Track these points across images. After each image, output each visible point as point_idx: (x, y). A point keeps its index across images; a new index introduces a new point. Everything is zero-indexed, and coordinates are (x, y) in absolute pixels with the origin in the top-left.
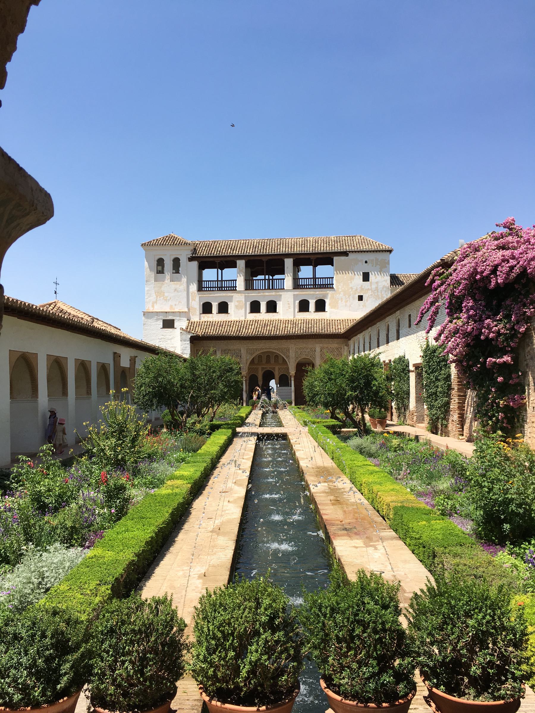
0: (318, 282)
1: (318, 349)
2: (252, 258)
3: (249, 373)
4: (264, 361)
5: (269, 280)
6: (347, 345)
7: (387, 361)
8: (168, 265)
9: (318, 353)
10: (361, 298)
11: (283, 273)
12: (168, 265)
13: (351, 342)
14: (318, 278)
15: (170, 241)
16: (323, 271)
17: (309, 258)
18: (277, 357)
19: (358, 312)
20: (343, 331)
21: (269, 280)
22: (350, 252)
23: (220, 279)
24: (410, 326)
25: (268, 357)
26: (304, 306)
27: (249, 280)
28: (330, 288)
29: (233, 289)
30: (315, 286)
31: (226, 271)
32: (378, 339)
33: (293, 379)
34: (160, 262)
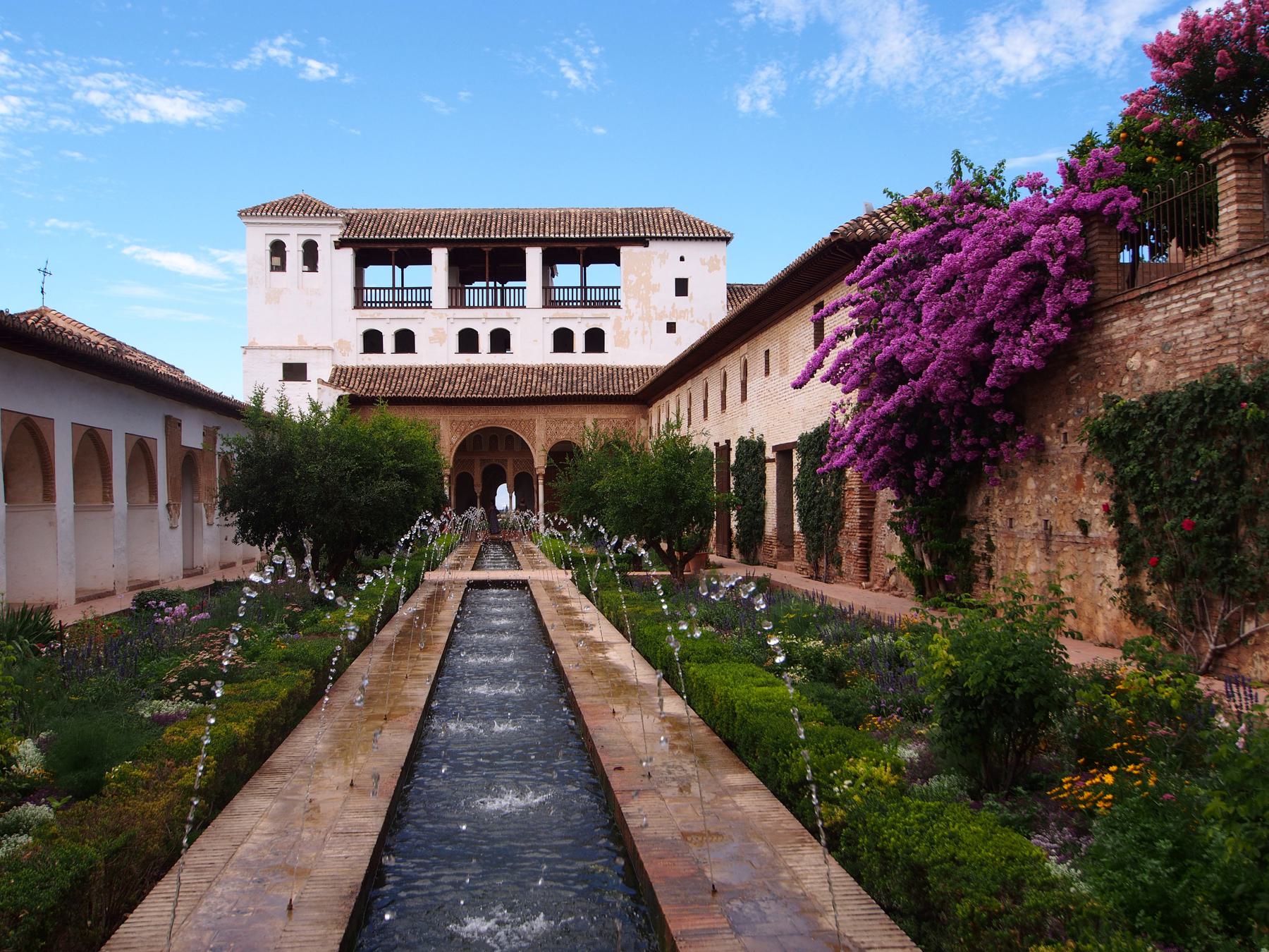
0: (591, 295)
5: (495, 288)
6: (646, 417)
7: (722, 443)
10: (671, 328)
13: (653, 410)
15: (300, 207)
16: (599, 274)
17: (574, 249)
19: (664, 353)
22: (651, 238)
23: (398, 284)
24: (767, 373)
26: (563, 340)
28: (613, 307)
29: (427, 305)
30: (585, 304)
31: (411, 270)
32: (705, 402)
33: (541, 481)
34: (278, 249)
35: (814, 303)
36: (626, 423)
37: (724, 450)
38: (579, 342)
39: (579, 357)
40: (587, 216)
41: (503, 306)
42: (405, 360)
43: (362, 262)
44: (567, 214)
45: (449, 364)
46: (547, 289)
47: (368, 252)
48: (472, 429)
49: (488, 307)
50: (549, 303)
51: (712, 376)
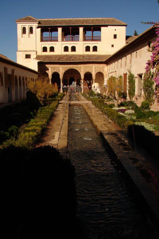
1: (94, 68)
8: (27, 31)
9: (94, 69)
10: (113, 46)
12: (27, 31)
14: (94, 37)
16: (96, 33)
19: (112, 52)
20: (105, 60)
23: (51, 36)
24: (136, 57)
26: (88, 49)
30: (93, 40)
31: (53, 33)
32: (121, 63)
35: (148, 41)
36: (102, 68)
37: (125, 75)
38: (91, 49)
39: (91, 53)
42: (52, 53)
43: (42, 31)
47: (44, 29)
48: (67, 69)
50: (85, 39)
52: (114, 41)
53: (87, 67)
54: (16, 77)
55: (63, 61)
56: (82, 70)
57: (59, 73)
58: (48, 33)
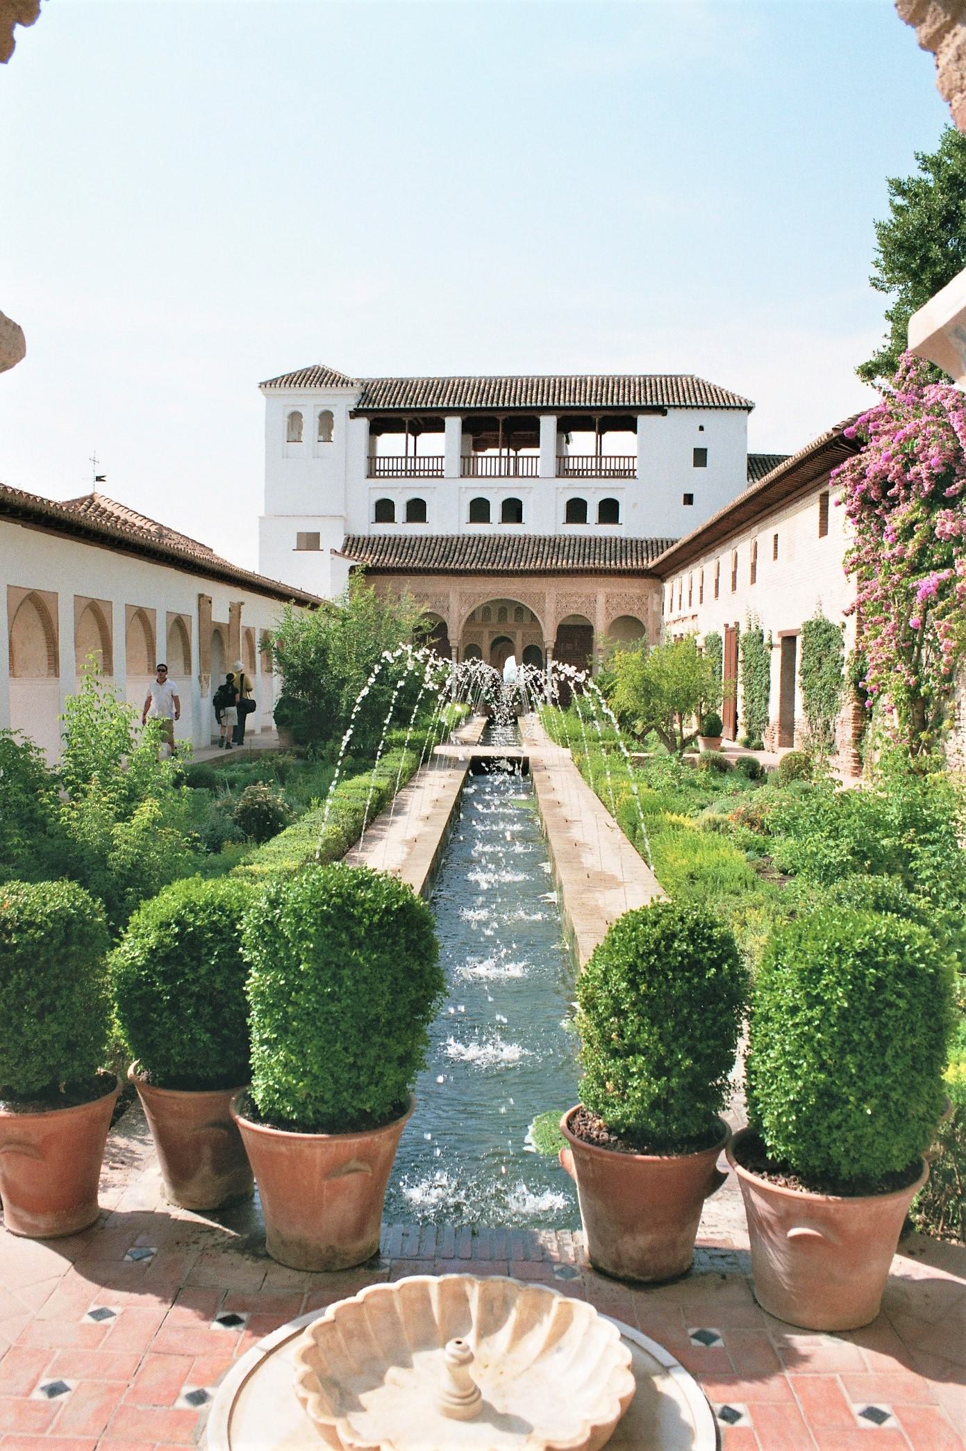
1: (601, 599)
2: (477, 414)
3: (463, 641)
4: (494, 619)
5: (509, 457)
6: (660, 592)
7: (732, 625)
10: (689, 499)
11: (535, 443)
13: (667, 586)
15: (318, 377)
16: (617, 442)
18: (520, 610)
20: (651, 565)
21: (509, 457)
23: (411, 453)
24: (775, 557)
25: (503, 612)
26: (576, 510)
27: (469, 458)
30: (601, 473)
31: (423, 437)
32: (717, 581)
35: (821, 492)
36: (639, 598)
37: (733, 632)
38: (592, 512)
39: (592, 528)
40: (603, 382)
41: (516, 475)
42: (416, 530)
44: (583, 380)
45: (461, 534)
46: (561, 458)
48: (482, 601)
49: (500, 476)
50: (563, 470)
51: (724, 556)
52: (696, 480)
53: (571, 595)
54: (249, 634)
55: (462, 566)
56: (551, 604)
57: (445, 616)
58: (401, 437)
